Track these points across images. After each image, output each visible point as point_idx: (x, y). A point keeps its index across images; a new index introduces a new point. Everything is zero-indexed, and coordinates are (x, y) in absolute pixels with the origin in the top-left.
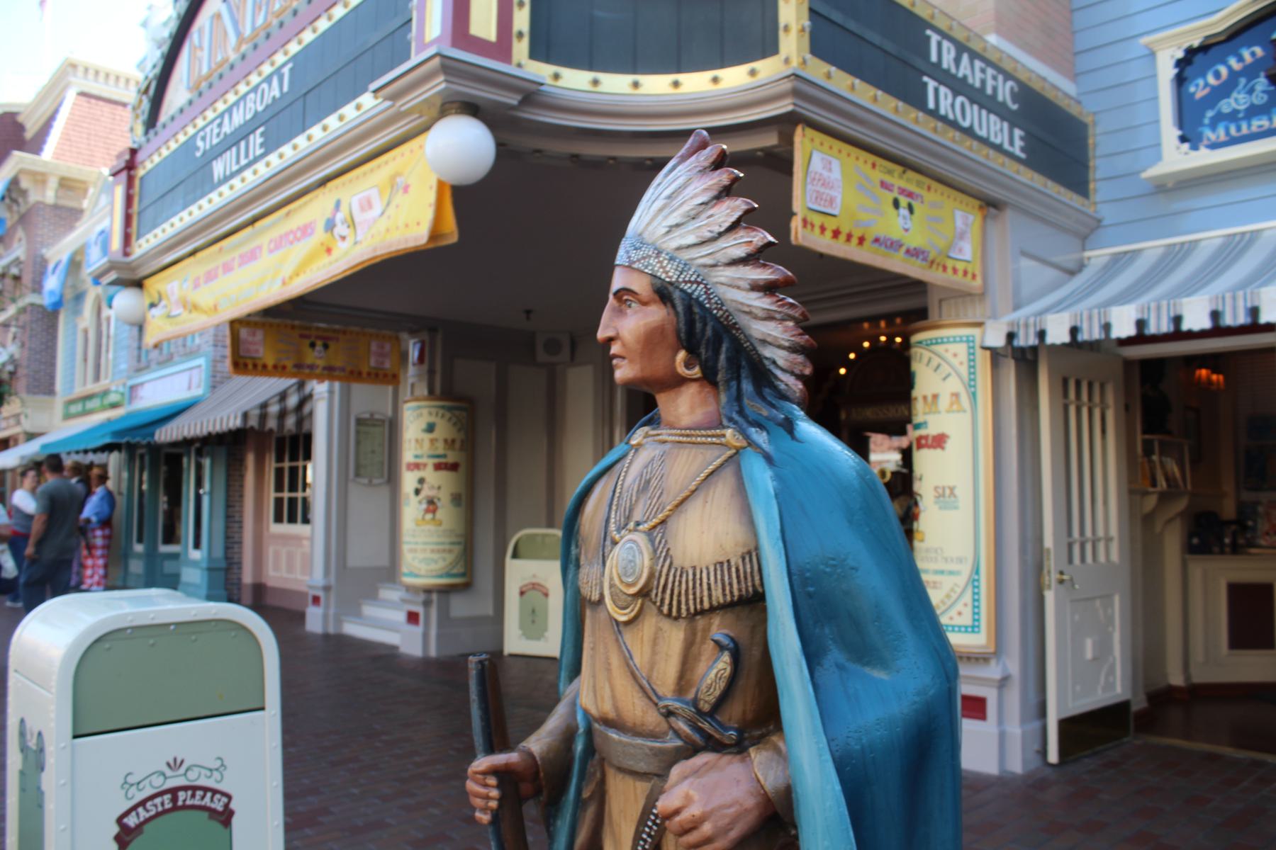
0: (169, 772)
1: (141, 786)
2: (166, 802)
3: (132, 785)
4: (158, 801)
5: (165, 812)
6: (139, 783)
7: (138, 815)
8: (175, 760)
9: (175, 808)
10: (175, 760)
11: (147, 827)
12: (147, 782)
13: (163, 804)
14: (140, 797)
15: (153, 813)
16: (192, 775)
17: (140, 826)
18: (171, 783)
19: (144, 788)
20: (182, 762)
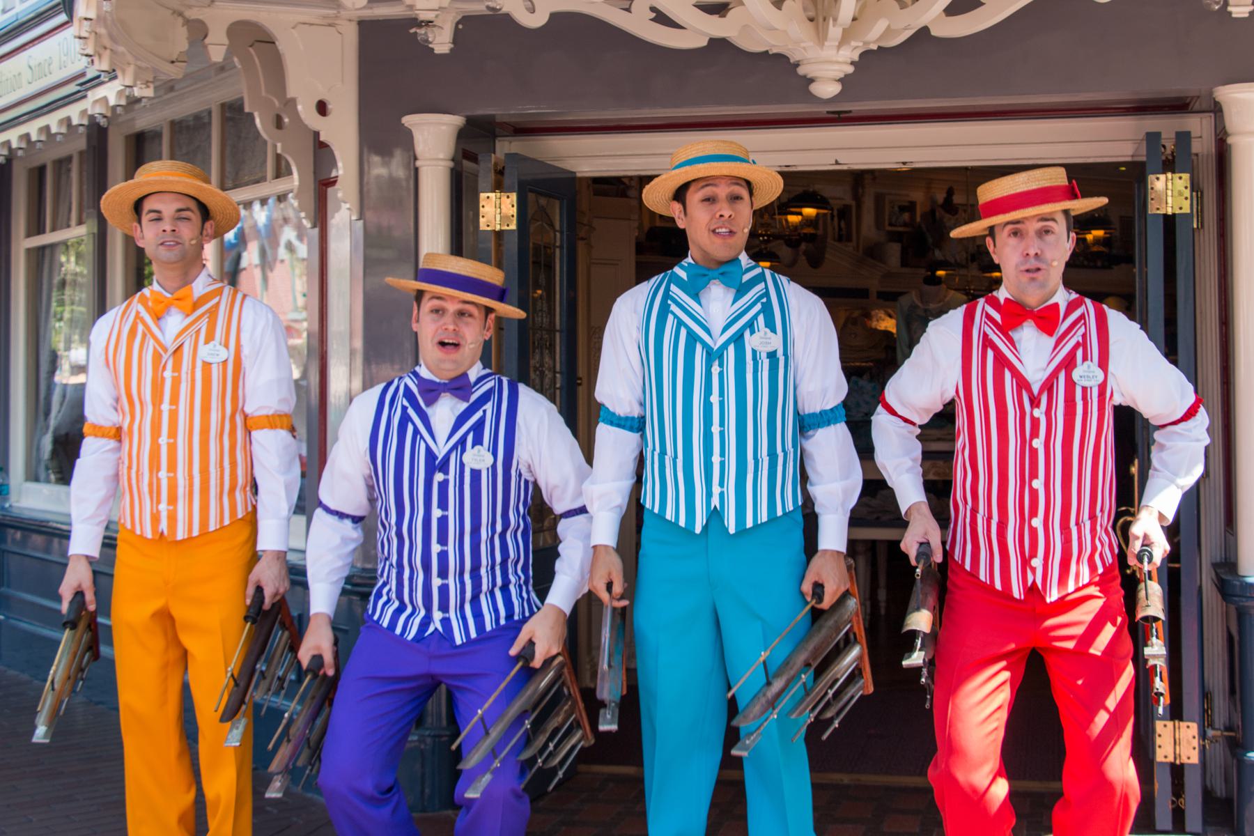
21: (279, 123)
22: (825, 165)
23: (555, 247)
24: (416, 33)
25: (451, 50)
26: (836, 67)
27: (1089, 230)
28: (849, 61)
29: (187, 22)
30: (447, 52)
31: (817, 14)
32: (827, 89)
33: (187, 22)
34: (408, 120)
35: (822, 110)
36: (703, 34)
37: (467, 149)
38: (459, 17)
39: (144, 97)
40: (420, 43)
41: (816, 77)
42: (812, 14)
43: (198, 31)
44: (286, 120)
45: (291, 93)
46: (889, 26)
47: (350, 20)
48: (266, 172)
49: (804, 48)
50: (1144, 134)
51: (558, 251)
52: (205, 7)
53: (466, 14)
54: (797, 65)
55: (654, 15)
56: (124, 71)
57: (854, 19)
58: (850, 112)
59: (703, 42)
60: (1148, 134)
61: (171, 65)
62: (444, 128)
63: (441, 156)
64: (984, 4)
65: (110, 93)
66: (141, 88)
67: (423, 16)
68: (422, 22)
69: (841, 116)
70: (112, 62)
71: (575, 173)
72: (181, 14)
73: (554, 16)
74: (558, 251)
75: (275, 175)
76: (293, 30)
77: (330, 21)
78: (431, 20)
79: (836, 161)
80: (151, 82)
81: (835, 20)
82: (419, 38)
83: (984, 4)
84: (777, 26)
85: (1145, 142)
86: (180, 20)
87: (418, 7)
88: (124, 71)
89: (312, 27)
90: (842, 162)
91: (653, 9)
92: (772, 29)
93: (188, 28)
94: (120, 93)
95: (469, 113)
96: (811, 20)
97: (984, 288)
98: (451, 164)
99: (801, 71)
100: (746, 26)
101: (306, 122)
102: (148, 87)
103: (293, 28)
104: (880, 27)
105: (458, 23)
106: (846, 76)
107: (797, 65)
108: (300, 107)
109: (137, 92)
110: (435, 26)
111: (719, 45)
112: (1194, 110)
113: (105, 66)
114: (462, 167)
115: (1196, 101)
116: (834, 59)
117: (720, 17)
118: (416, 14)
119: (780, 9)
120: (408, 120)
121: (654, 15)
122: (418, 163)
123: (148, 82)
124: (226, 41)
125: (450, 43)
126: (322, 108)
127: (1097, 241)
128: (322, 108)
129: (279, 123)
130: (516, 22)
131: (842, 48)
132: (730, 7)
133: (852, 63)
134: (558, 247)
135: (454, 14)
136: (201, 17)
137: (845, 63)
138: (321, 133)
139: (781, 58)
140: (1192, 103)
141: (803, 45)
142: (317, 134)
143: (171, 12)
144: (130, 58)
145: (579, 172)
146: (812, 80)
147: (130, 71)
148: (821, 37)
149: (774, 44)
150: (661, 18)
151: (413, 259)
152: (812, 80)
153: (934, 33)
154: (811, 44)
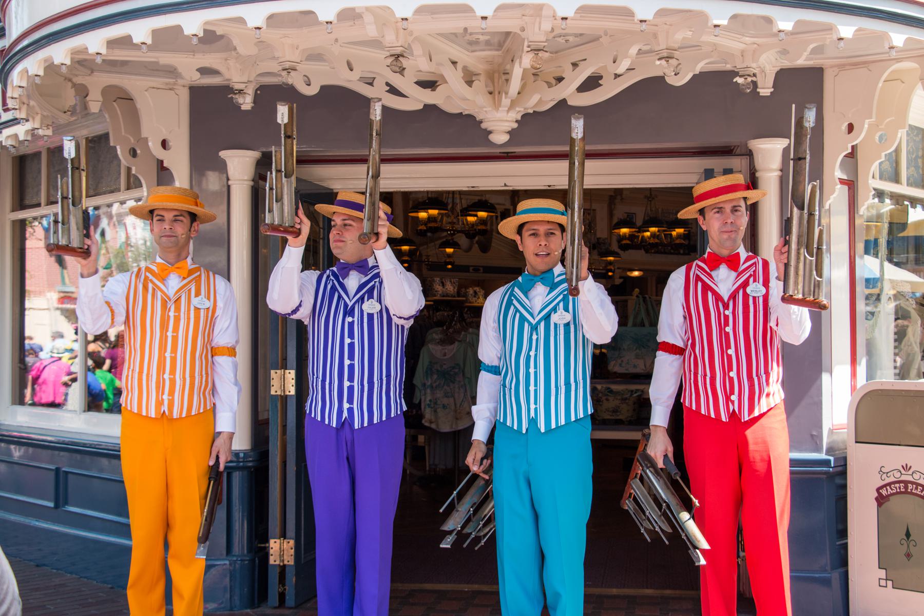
0: (903, 472)
1: (889, 475)
2: (902, 487)
3: (884, 473)
4: (897, 485)
5: (901, 493)
6: (887, 473)
7: (887, 490)
8: (907, 465)
9: (906, 492)
10: (907, 465)
11: (891, 498)
12: (892, 473)
13: (900, 488)
14: (888, 480)
15: (895, 491)
16: (916, 476)
17: (888, 496)
18: (904, 478)
19: (890, 476)
20: (910, 467)
21: (134, 153)
22: (498, 187)
23: (320, 238)
24: (232, 97)
25: (252, 107)
26: (507, 124)
27: (674, 228)
28: (515, 121)
29: (74, 85)
30: (250, 109)
31: (494, 90)
32: (500, 138)
33: (74, 85)
34: (223, 154)
35: (497, 151)
36: (421, 101)
37: (261, 173)
38: (258, 86)
39: (45, 136)
40: (235, 104)
41: (493, 130)
42: (491, 89)
43: (83, 92)
44: (138, 152)
45: (144, 135)
46: (541, 98)
47: (184, 86)
48: (120, 185)
49: (486, 111)
50: (703, 169)
51: (321, 241)
52: (86, 76)
53: (262, 84)
54: (481, 122)
55: (388, 88)
56: (34, 118)
57: (519, 93)
58: (515, 152)
59: (421, 107)
60: (705, 170)
61: (64, 115)
62: (248, 159)
63: (246, 178)
64: (602, 85)
65: (21, 130)
66: (44, 129)
67: (237, 87)
68: (236, 90)
69: (509, 155)
70: (28, 114)
71: (332, 189)
72: (70, 80)
73: (323, 88)
74: (321, 241)
75: (126, 188)
76: (145, 92)
77: (171, 87)
78: (242, 89)
79: (505, 184)
80: (51, 125)
81: (507, 93)
82: (234, 101)
83: (602, 85)
84: (469, 98)
85: (704, 174)
86: (70, 84)
87: (234, 81)
88: (34, 118)
89: (159, 90)
90: (509, 185)
91: (387, 84)
92: (465, 99)
93: (75, 90)
94: (27, 132)
95: (264, 150)
96: (491, 93)
97: (601, 268)
98: (252, 183)
99: (483, 126)
100: (449, 97)
101: (153, 153)
102: (48, 129)
103: (146, 91)
104: (535, 99)
105: (257, 90)
106: (513, 129)
107: (481, 122)
108: (150, 144)
109: (41, 132)
110: (245, 93)
111: (430, 109)
112: (736, 153)
113: (23, 115)
114: (259, 186)
115: (737, 149)
116: (505, 119)
117: (431, 91)
118: (233, 85)
119: (471, 87)
120: (223, 154)
121: (388, 88)
122: (230, 183)
123: (48, 125)
124: (101, 99)
125: (251, 103)
126: (164, 144)
127: (679, 236)
128: (164, 144)
129: (134, 153)
130: (298, 92)
131: (511, 112)
132: (438, 84)
133: (517, 121)
134: (321, 239)
135: (255, 84)
136: (84, 82)
137: (512, 121)
138: (164, 161)
139: (471, 117)
140: (735, 151)
141: (485, 109)
142: (162, 162)
143: (64, 78)
144: (38, 109)
145: (335, 189)
146: (490, 132)
147: (38, 118)
148: (497, 105)
149: (466, 109)
150: (393, 90)
151: (226, 246)
152: (490, 132)
153: (570, 103)
154: (490, 109)
